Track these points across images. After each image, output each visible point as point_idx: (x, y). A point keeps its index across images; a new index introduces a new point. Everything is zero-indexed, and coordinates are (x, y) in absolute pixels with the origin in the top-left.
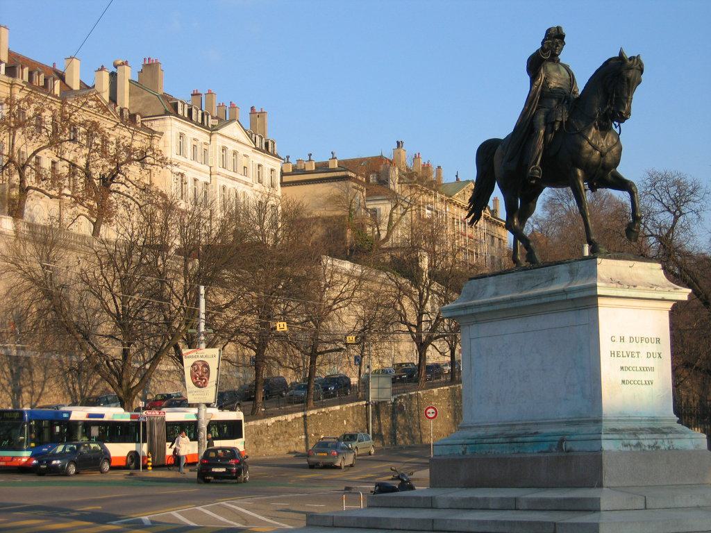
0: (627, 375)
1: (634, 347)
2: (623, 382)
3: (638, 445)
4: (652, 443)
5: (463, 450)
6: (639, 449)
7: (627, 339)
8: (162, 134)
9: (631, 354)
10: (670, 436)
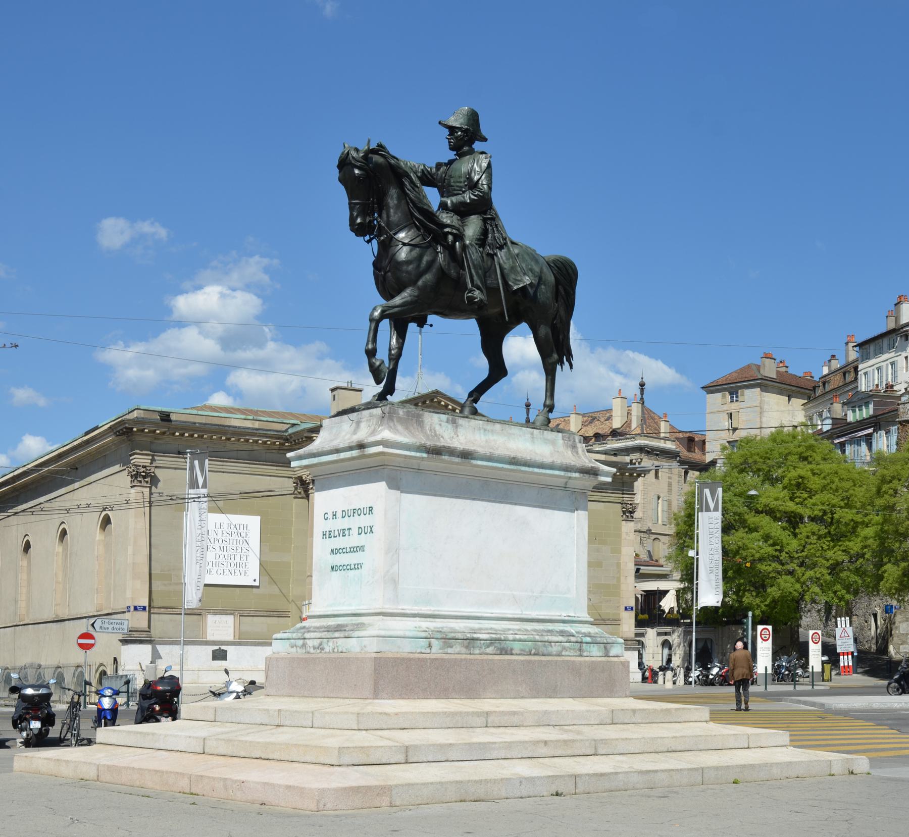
0: (340, 559)
3: (304, 645)
7: (339, 514)
9: (343, 533)
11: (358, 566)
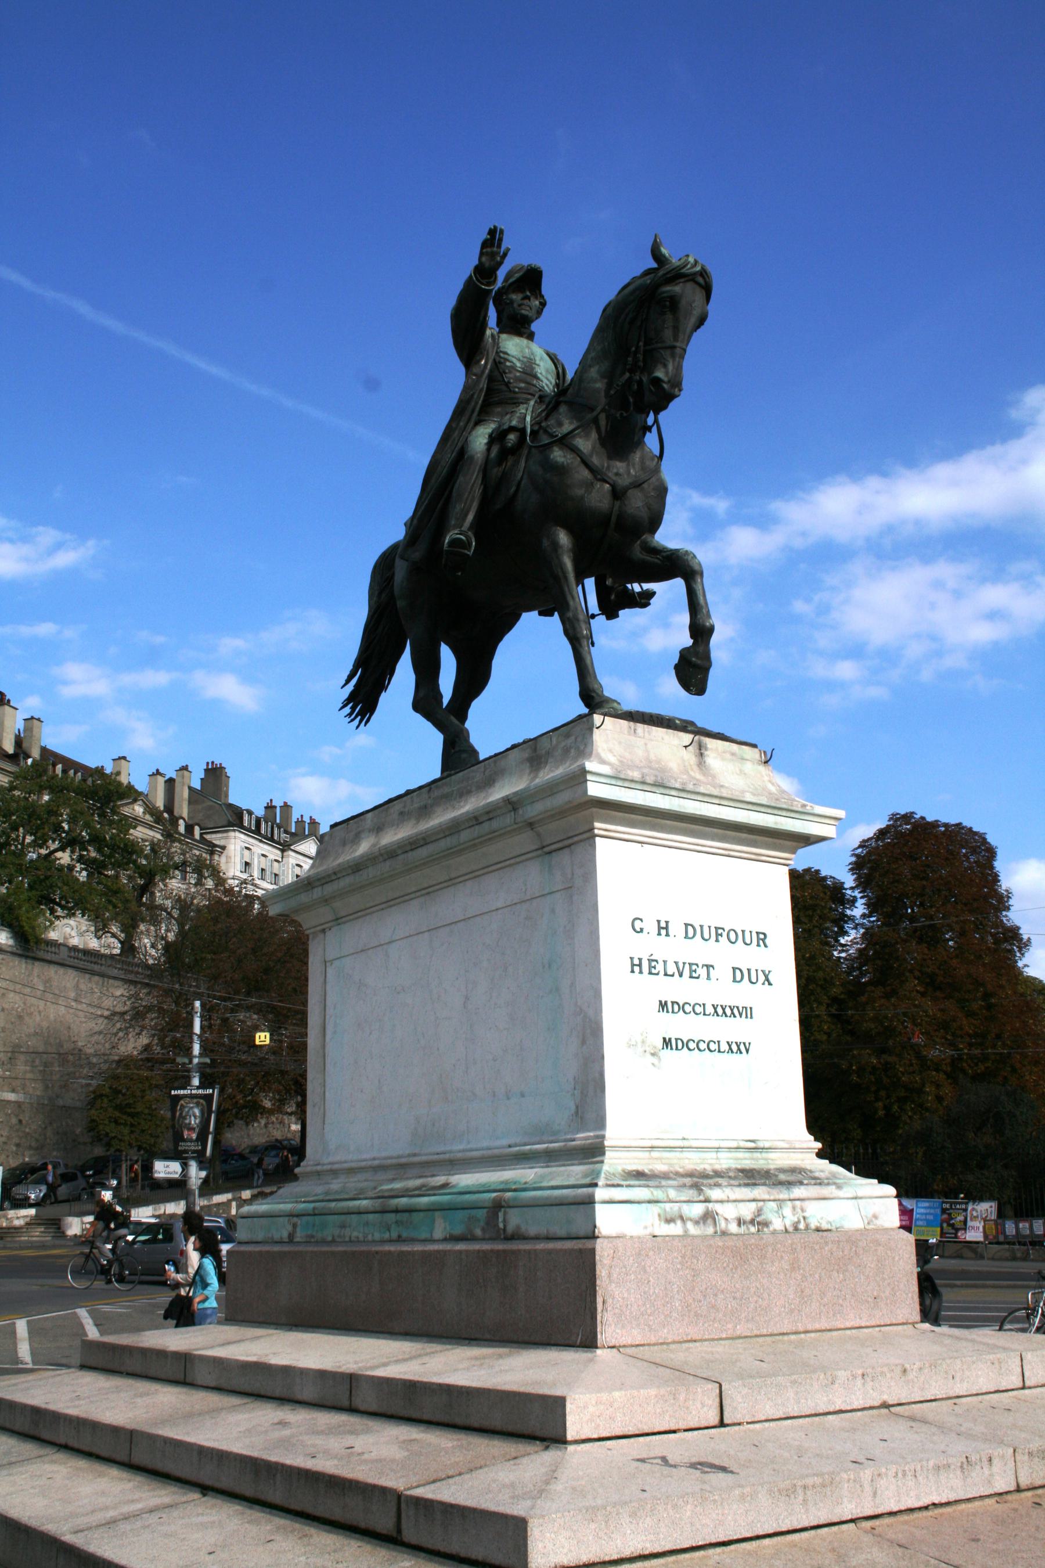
1: (698, 951)
2: (667, 1042)
3: (708, 1217)
4: (747, 1211)
5: (290, 1228)
6: (710, 1230)
7: (677, 928)
8: (224, 848)
10: (798, 1192)
11: (740, 1048)
